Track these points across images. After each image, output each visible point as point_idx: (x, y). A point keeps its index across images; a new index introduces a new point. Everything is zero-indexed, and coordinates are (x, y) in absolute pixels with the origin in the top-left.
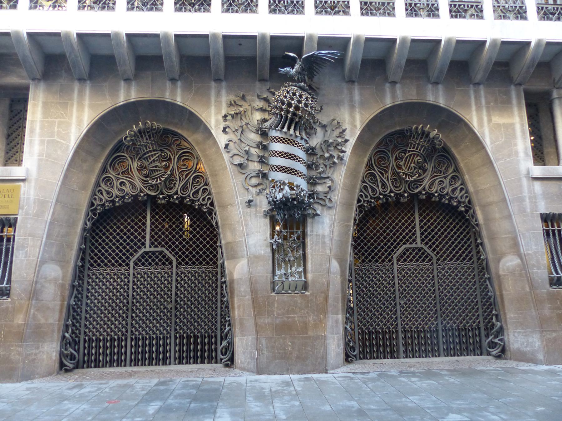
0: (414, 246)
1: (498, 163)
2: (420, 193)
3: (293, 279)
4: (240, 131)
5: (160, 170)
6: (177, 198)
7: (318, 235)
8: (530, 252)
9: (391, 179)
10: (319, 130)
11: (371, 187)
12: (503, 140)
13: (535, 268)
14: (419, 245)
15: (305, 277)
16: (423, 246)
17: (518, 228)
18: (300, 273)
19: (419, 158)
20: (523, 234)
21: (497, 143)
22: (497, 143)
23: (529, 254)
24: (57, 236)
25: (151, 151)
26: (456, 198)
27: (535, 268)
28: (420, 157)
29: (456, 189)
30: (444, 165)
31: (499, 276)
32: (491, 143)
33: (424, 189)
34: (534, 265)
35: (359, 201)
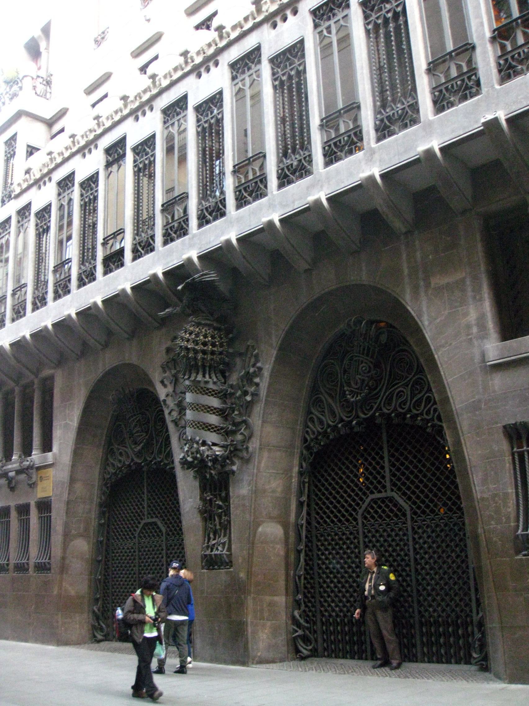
0: (383, 495)
1: (440, 353)
2: (373, 415)
3: (216, 552)
4: (174, 382)
5: (141, 435)
6: (155, 463)
7: (238, 496)
8: (486, 496)
9: (340, 402)
10: (238, 361)
11: (319, 419)
12: (447, 312)
13: (493, 522)
14: (389, 494)
15: (229, 549)
16: (394, 494)
17: (468, 455)
18: (224, 544)
19: (364, 364)
20: (474, 466)
21: (438, 321)
22: (438, 321)
23: (483, 499)
24: (83, 513)
25: (132, 417)
26: (422, 414)
27: (493, 522)
28: (365, 363)
29: (421, 398)
30: (407, 365)
31: (476, 537)
32: (430, 323)
33: (379, 409)
34: (491, 517)
35: (305, 440)
